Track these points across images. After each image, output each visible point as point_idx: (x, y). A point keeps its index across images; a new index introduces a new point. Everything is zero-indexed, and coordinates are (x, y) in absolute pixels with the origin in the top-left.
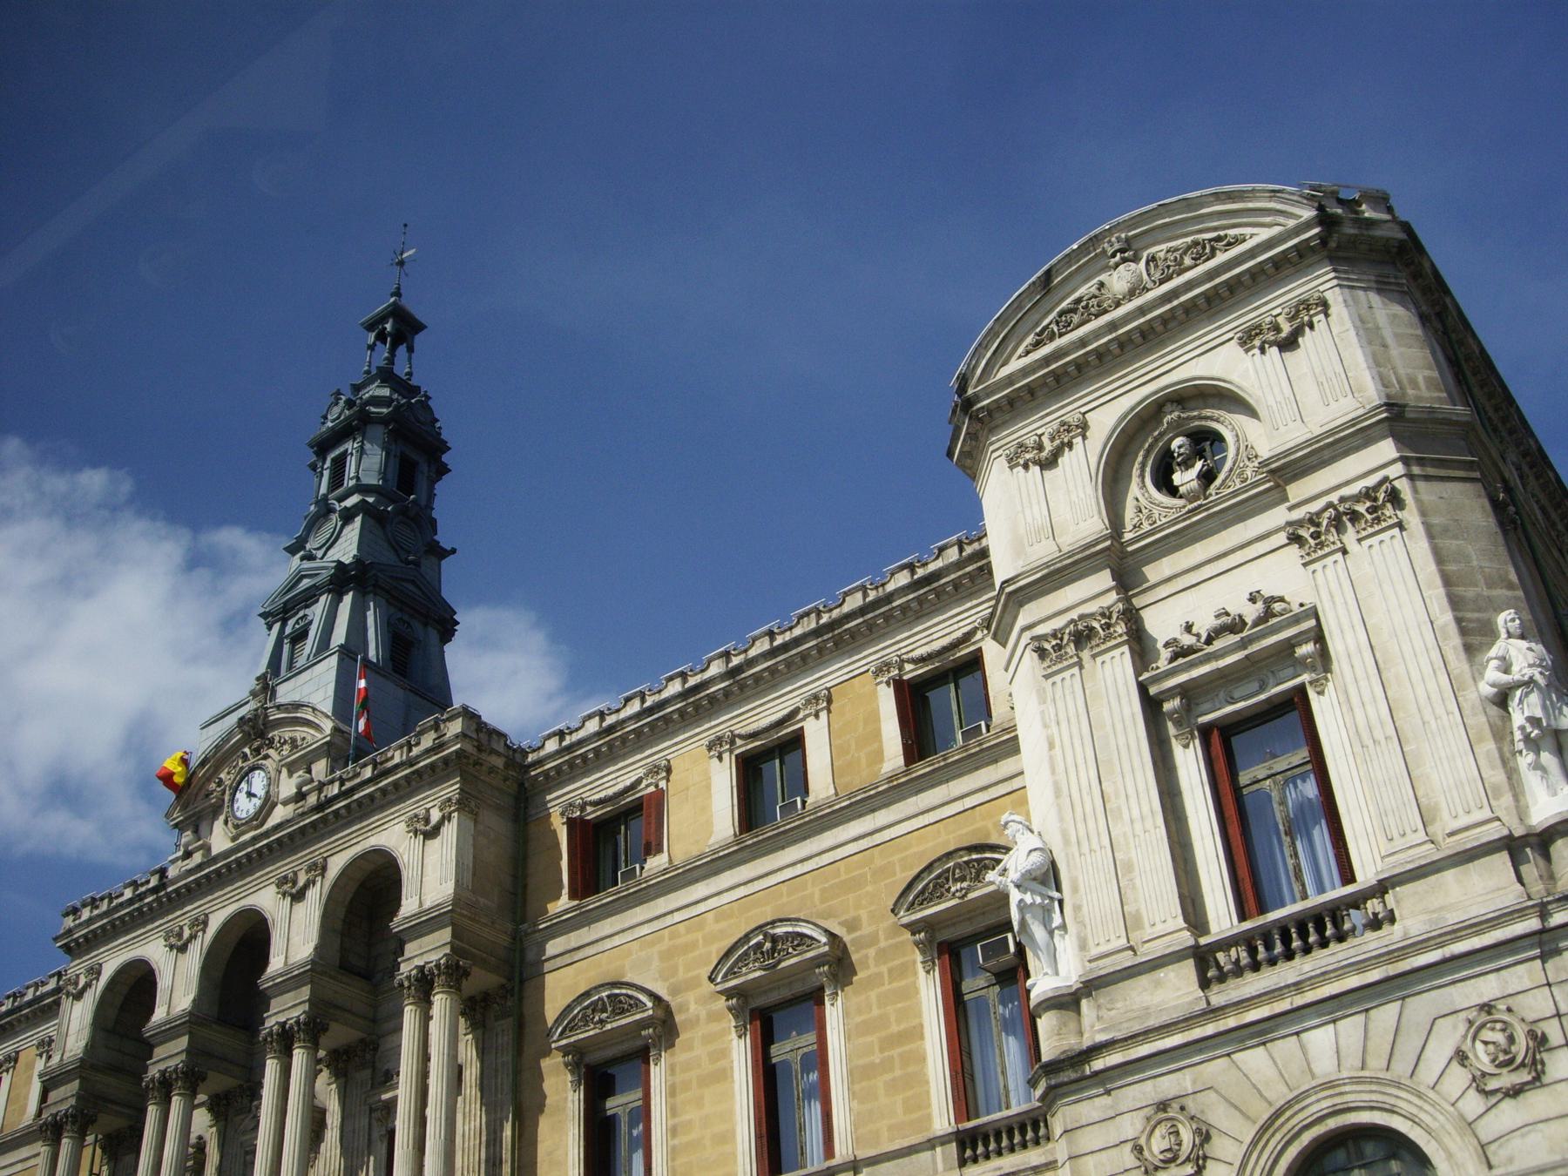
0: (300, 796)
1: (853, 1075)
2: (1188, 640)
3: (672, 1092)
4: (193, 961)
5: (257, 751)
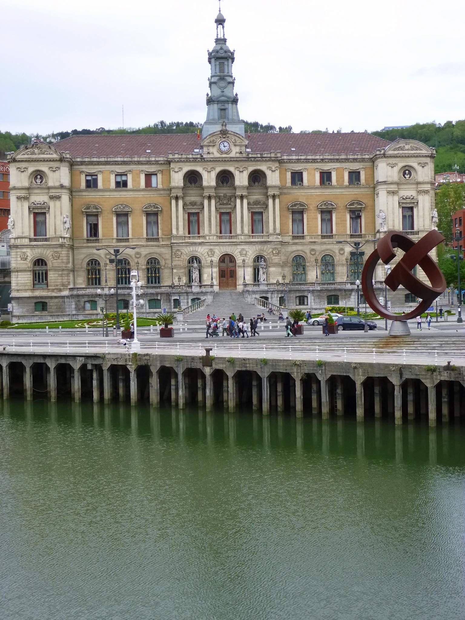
0: (241, 153)
1: (336, 224)
2: (404, 198)
3: (308, 219)
4: (213, 175)
5: (224, 138)
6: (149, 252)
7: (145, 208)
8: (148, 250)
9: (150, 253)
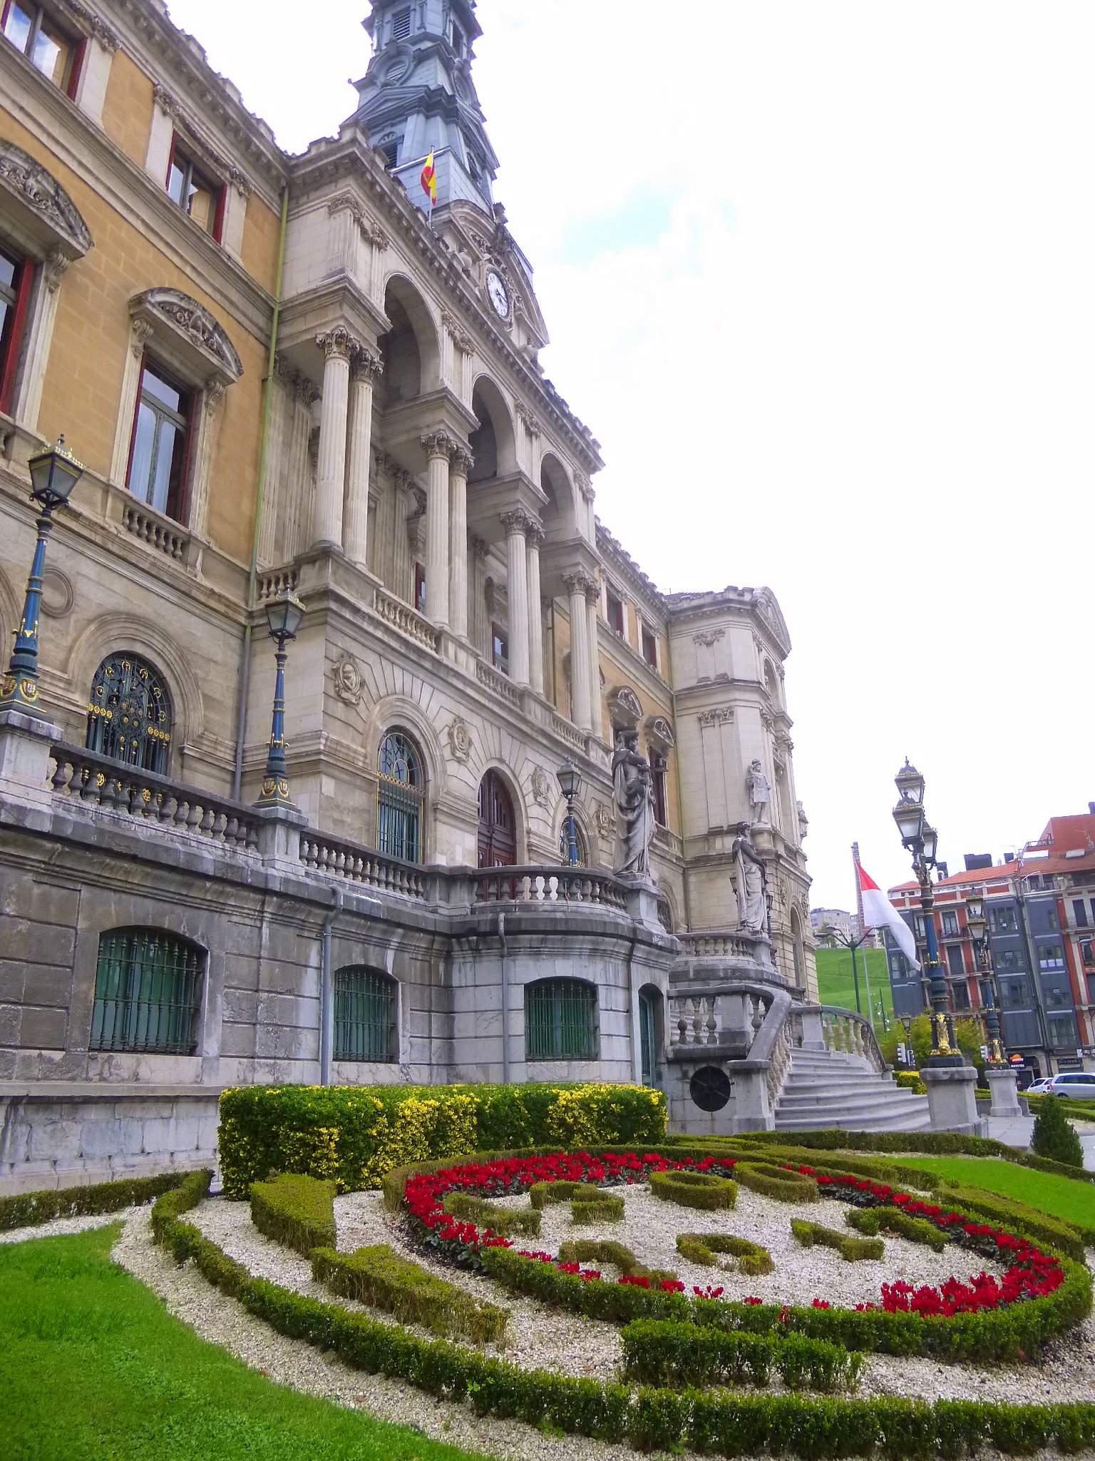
6: (123, 606)
7: (162, 305)
8: (119, 585)
9: (132, 618)
